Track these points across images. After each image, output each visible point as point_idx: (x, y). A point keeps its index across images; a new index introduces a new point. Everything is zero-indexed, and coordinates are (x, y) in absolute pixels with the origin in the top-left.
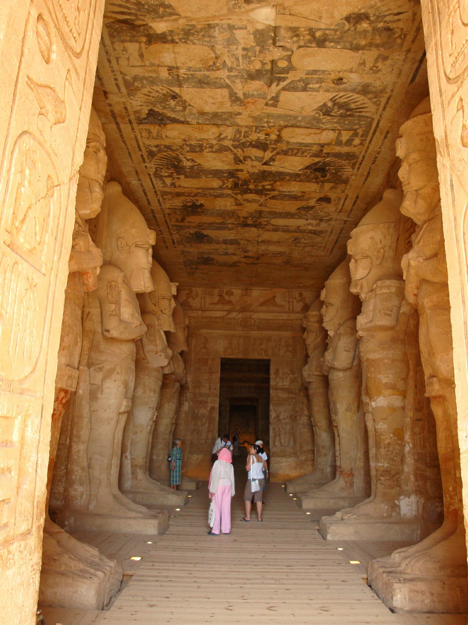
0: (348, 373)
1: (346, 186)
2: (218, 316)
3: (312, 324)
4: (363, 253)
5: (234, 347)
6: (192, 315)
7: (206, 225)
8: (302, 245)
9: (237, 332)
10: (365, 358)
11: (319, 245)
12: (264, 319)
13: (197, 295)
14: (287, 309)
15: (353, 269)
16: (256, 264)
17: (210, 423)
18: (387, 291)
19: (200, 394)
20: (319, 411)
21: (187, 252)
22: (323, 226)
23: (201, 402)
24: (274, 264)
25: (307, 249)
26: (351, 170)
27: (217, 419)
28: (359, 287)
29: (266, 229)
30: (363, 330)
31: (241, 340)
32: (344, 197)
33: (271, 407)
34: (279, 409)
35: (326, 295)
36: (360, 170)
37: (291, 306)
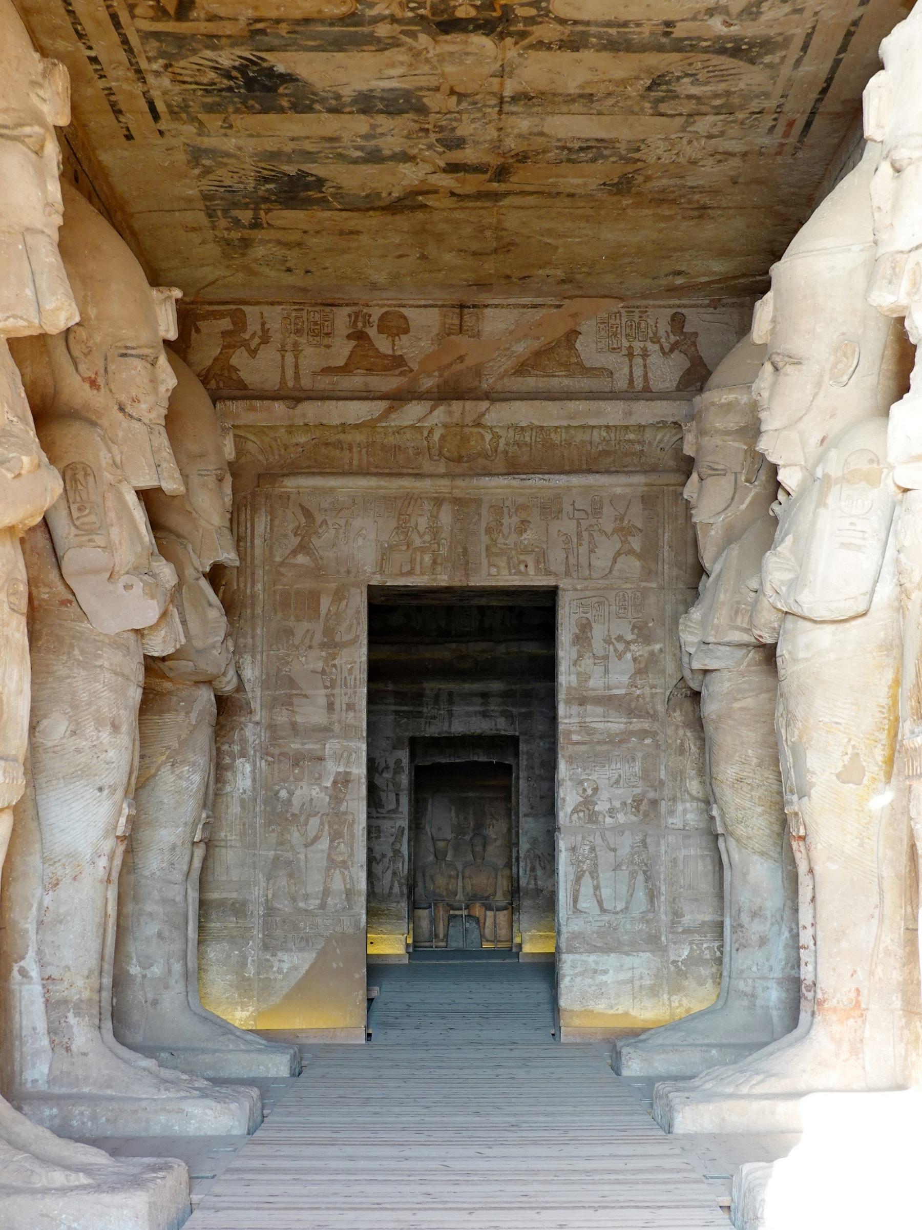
2: (351, 421)
3: (718, 440)
6: (248, 418)
7: (283, 29)
8: (688, 107)
11: (755, 105)
12: (531, 427)
13: (265, 340)
14: (622, 384)
16: (496, 196)
17: (335, 837)
21: (211, 152)
25: (703, 125)
27: (364, 816)
35: (774, 321)
37: (638, 372)
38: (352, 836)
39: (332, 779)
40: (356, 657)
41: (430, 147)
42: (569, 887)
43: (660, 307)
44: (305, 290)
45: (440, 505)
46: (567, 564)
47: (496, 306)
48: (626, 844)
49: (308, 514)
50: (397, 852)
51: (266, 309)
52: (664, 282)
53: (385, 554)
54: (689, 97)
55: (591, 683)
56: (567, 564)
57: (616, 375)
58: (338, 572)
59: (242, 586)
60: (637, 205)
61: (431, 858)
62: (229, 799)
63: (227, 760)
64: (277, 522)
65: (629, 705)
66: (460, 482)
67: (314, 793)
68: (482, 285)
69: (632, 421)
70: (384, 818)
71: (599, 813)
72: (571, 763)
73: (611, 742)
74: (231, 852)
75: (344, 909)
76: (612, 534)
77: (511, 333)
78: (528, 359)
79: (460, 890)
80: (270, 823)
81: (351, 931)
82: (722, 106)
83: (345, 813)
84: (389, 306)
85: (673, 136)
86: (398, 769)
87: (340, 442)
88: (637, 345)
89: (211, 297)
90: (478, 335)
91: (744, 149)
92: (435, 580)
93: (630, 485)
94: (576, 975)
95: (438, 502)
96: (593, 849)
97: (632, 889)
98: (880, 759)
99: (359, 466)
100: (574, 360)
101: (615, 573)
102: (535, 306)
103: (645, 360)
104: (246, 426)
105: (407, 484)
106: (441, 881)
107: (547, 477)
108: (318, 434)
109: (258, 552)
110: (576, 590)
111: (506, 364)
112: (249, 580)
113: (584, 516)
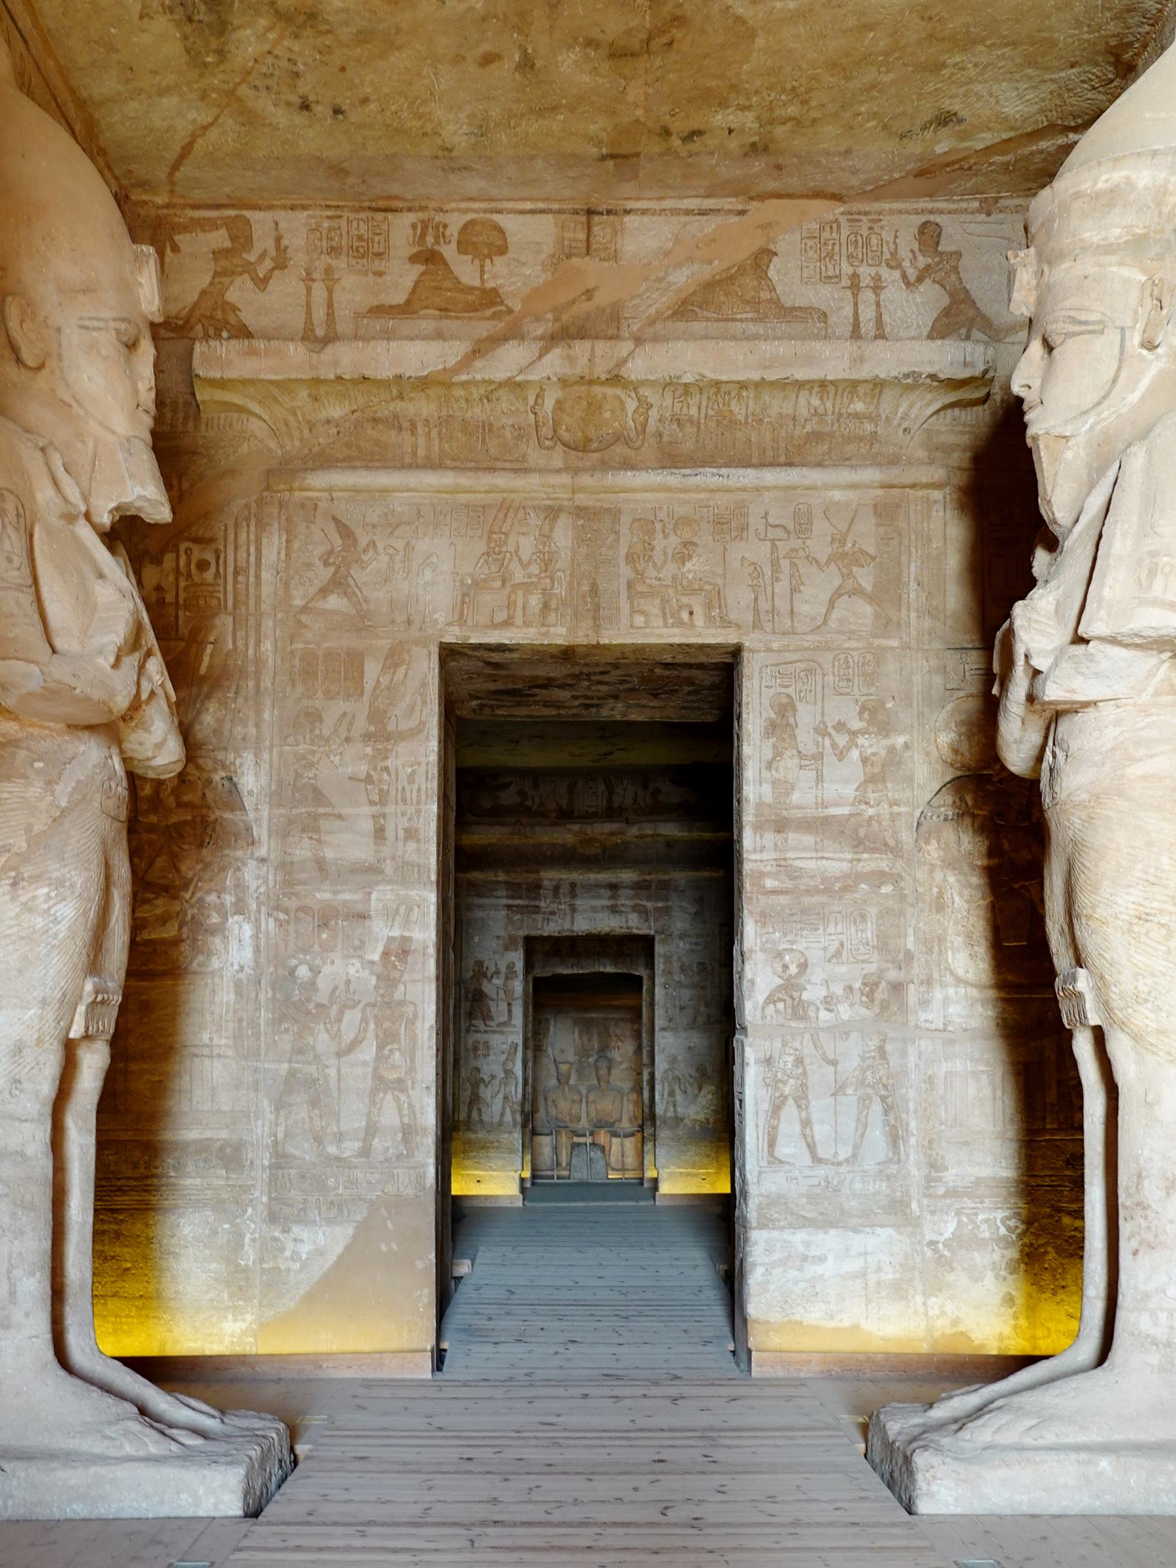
5: (519, 575)
9: (535, 480)
19: (321, 865)
20: (1144, 918)
23: (325, 918)
31: (563, 535)
33: (751, 933)
34: (800, 946)
38: (413, 1039)
39: (380, 949)
40: (421, 758)
42: (761, 1122)
43: (901, 212)
44: (338, 171)
45: (555, 518)
46: (756, 610)
47: (644, 212)
48: (852, 1053)
49: (346, 533)
50: (508, 1073)
51: (282, 216)
53: (467, 595)
57: (833, 319)
58: (393, 622)
59: (240, 643)
61: (553, 1082)
62: (217, 980)
63: (215, 919)
64: (296, 545)
65: (856, 831)
66: (586, 480)
67: (352, 971)
68: (620, 159)
70: (493, 1032)
71: (810, 1003)
72: (764, 925)
74: (218, 1064)
75: (399, 1157)
76: (828, 563)
77: (667, 254)
78: (694, 293)
79: (584, 1115)
80: (282, 1018)
81: (409, 1192)
83: (402, 1003)
84: (475, 211)
86: (511, 973)
87: (396, 416)
89: (196, 195)
90: (616, 257)
92: (545, 635)
93: (853, 486)
94: (774, 1265)
95: (552, 513)
96: (799, 1061)
97: (863, 1126)
99: (427, 457)
100: (765, 295)
101: (832, 624)
102: (703, 213)
103: (877, 295)
104: (245, 382)
105: (501, 480)
106: (563, 1105)
107: (724, 471)
108: (361, 401)
109: (266, 590)
110: (770, 650)
111: (661, 302)
112: (253, 634)
113: (784, 535)
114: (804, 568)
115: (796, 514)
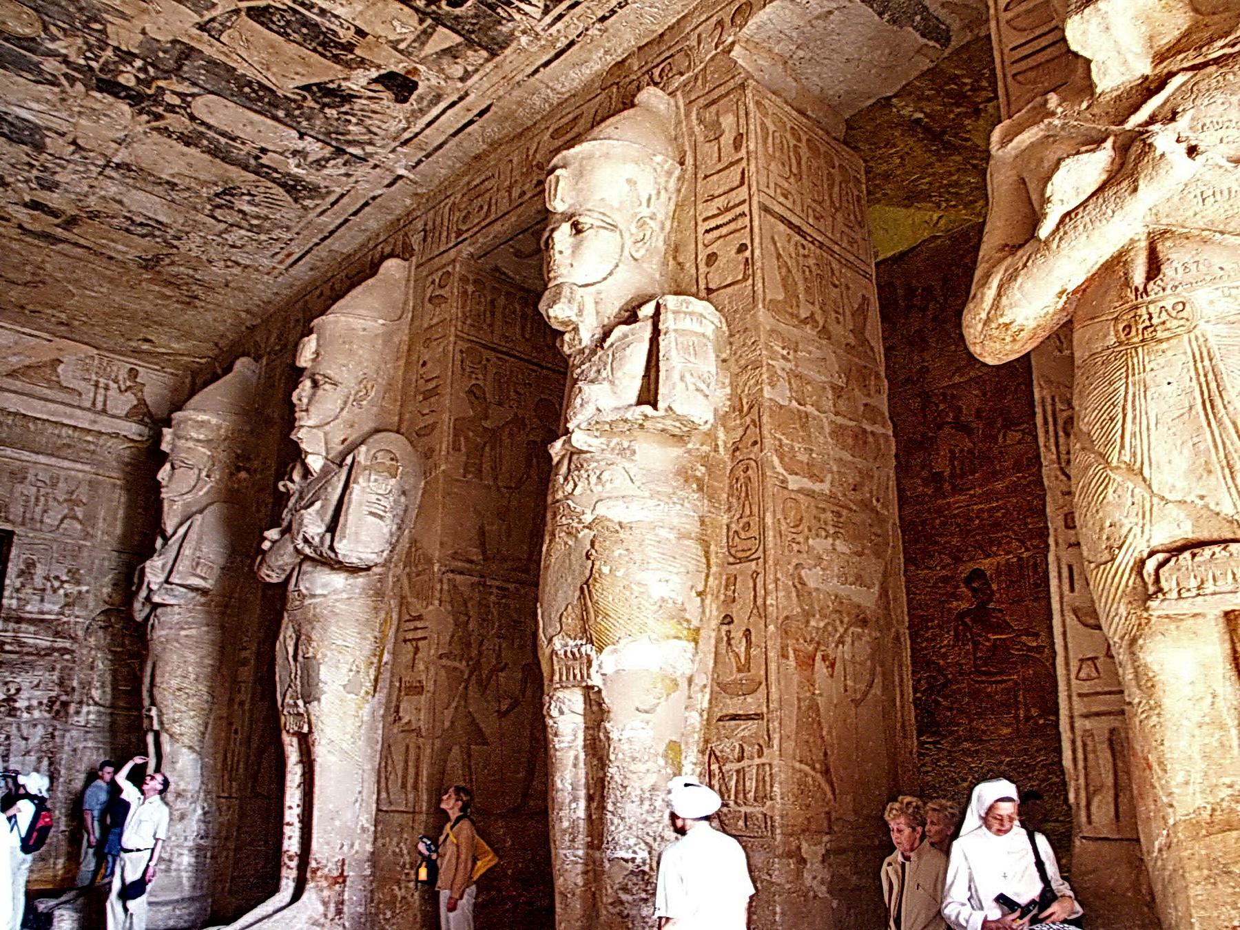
0: (361, 580)
1: (487, 60)
3: (191, 444)
4: (604, 214)
10: (588, 518)
12: (16, 414)
15: (567, 252)
18: (696, 327)
22: (334, 169)
24: (111, 258)
26: (536, 13)
28: (576, 310)
29: (161, 124)
30: (594, 426)
32: (455, 98)
35: (317, 353)
36: (559, 25)
37: (100, 398)
41: (27, 181)
52: (134, 344)
54: (240, 211)
55: (28, 608)
56: (24, 517)
60: (151, 281)
69: (96, 428)
73: (38, 654)
82: (256, 226)
85: (210, 237)
88: (102, 381)
91: (248, 262)
98: (372, 677)
114: (51, 502)
115: (51, 478)
